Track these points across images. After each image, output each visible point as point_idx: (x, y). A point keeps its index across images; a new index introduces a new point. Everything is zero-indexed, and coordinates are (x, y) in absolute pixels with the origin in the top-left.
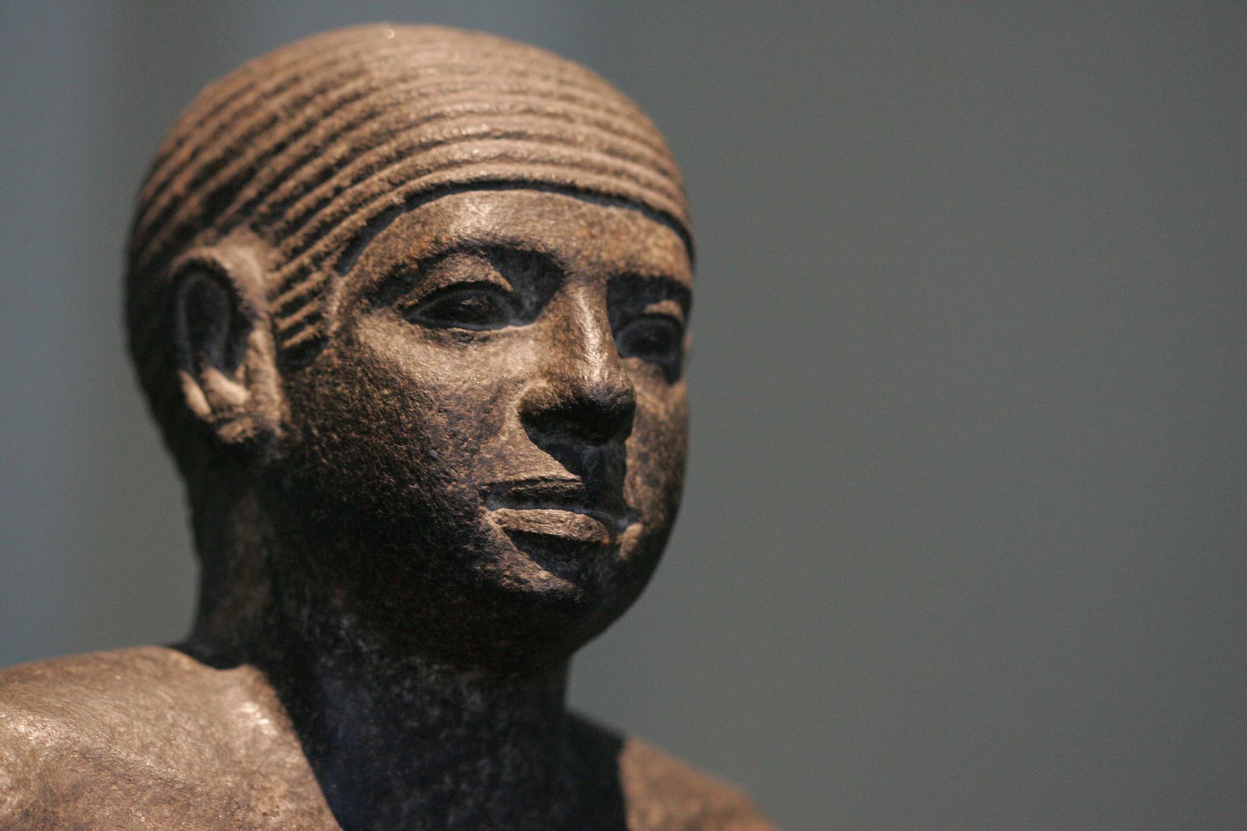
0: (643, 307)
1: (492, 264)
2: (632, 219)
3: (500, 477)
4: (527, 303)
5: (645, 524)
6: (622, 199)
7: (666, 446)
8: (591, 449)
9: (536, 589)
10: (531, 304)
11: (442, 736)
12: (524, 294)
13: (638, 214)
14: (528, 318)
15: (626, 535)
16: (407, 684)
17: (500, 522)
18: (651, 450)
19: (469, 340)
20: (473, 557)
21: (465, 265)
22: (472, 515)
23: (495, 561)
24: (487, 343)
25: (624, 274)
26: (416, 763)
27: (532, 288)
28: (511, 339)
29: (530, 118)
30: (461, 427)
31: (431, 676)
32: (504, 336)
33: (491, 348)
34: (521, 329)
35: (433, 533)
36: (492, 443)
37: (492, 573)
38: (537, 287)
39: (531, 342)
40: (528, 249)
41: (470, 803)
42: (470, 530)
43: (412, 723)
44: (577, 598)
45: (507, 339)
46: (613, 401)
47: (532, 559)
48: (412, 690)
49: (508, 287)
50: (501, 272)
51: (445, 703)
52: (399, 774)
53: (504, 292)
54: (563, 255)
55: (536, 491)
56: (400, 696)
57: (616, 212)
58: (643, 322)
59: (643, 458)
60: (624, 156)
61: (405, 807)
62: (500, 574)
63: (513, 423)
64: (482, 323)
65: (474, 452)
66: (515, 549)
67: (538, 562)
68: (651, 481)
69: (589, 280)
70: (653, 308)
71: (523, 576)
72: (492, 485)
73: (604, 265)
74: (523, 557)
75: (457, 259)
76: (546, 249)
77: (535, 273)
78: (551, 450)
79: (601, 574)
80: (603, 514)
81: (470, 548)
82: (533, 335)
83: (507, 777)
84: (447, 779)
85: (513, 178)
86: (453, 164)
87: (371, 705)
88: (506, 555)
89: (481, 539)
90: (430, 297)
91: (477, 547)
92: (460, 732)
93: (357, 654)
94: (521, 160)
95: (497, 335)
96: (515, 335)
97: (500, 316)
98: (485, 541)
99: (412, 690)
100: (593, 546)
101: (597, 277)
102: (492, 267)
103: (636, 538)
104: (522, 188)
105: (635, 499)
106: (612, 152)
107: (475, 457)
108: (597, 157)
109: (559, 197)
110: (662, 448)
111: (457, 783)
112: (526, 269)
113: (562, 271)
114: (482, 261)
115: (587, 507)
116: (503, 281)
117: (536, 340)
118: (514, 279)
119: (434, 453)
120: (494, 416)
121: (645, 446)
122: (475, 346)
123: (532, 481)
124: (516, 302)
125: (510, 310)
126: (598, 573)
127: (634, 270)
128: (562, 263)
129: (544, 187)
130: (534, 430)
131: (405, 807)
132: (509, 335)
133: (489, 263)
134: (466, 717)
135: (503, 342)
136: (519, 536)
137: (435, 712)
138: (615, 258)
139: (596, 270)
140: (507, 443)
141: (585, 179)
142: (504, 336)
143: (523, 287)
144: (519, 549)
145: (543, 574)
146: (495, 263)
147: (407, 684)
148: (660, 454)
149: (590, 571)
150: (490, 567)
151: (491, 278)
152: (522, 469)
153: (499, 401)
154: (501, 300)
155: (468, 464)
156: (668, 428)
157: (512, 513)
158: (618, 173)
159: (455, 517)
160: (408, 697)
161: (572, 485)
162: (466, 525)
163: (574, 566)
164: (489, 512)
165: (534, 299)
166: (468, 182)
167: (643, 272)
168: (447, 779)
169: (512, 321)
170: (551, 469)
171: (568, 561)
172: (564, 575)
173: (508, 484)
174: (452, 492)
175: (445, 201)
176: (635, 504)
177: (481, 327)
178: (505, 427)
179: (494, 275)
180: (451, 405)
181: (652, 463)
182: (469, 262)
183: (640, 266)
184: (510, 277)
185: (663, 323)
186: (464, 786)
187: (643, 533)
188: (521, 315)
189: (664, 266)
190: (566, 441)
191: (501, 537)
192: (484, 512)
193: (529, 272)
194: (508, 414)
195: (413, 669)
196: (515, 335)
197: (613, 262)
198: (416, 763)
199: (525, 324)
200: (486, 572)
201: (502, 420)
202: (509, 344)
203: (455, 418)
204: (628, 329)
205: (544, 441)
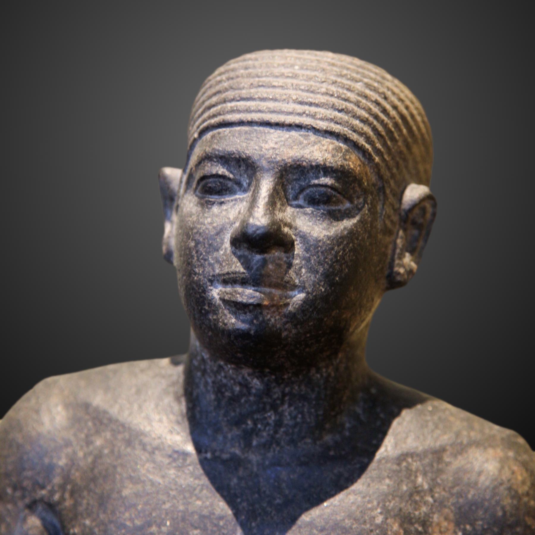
0: (310, 181)
1: (221, 165)
2: (306, 137)
3: (217, 271)
4: (245, 184)
5: (308, 293)
6: (299, 127)
7: (322, 252)
8: (258, 257)
9: (230, 328)
10: (246, 183)
11: (243, 401)
12: (242, 179)
13: (311, 133)
14: (245, 191)
15: (295, 299)
16: (223, 374)
17: (218, 294)
18: (311, 255)
19: (213, 203)
20: (207, 312)
21: (208, 166)
22: (204, 291)
23: (216, 314)
24: (223, 205)
25: (291, 165)
26: (233, 414)
27: (246, 176)
28: (236, 202)
29: (261, 89)
30: (201, 249)
31: (230, 369)
32: (232, 201)
33: (224, 207)
34: (241, 197)
35: (193, 301)
36: (215, 254)
37: (215, 320)
38: (247, 175)
39: (245, 203)
40: (238, 156)
41: (265, 434)
42: (204, 299)
43: (228, 394)
44: (252, 332)
45: (234, 202)
46: (255, 232)
47: (230, 313)
48: (225, 377)
49: (231, 176)
50: (227, 169)
51: (240, 384)
52: (225, 419)
53: (229, 179)
54: (256, 158)
55: (230, 279)
56: (221, 380)
57: (294, 133)
58: (311, 189)
59: (308, 260)
60: (311, 104)
61: (229, 436)
62: (217, 320)
63: (227, 244)
64: (219, 195)
65: (205, 260)
66: (224, 308)
67: (232, 314)
68: (312, 270)
69: (268, 170)
70: (316, 182)
71: (226, 321)
72: (213, 276)
73: (277, 162)
74: (226, 312)
75: (205, 164)
76: (246, 155)
77: (245, 168)
78: (239, 258)
79: (273, 320)
80: (267, 290)
81: (206, 308)
82: (246, 200)
83: (287, 420)
84: (249, 422)
85: (237, 121)
86: (214, 116)
87: (211, 384)
88: (220, 311)
89: (210, 303)
90: (198, 183)
91: (209, 307)
92: (252, 398)
93: (203, 360)
94: (248, 111)
95: (229, 201)
96: (238, 200)
97: (230, 191)
98: (212, 304)
99: (225, 377)
100: (259, 306)
101: (274, 168)
102: (221, 167)
103: (301, 300)
104: (242, 126)
105: (300, 281)
106: (301, 103)
107: (207, 263)
108: (291, 107)
109: (261, 128)
110: (320, 254)
111: (255, 424)
112: (240, 167)
113: (254, 167)
114: (215, 164)
115: (254, 286)
116: (227, 173)
117: (247, 202)
118: (236, 171)
119: (190, 260)
120: (217, 242)
121: (308, 253)
122: (216, 207)
123: (228, 273)
124: (239, 184)
125: (236, 187)
126: (269, 320)
127: (298, 163)
128: (253, 163)
129: (253, 124)
130: (234, 248)
131: (229, 436)
132: (236, 200)
133: (220, 165)
134: (254, 391)
135: (231, 204)
136: (223, 300)
137: (237, 389)
138: (285, 158)
139: (272, 165)
140: (223, 255)
141: (274, 118)
142: (232, 201)
143: (241, 175)
144: (225, 308)
145: (233, 320)
146: (223, 165)
147: (223, 374)
148: (318, 257)
149: (261, 319)
150: (215, 317)
151: (220, 173)
152: (226, 267)
153: (221, 234)
154: (230, 184)
155: (202, 265)
156: (324, 243)
157: (224, 290)
158: (300, 114)
159: (198, 292)
160: (224, 381)
161: (243, 276)
162: (203, 297)
163: (249, 316)
164: (214, 290)
165: (248, 181)
166: (217, 125)
167: (304, 163)
168: (249, 422)
169: (238, 193)
170: (238, 267)
171: (245, 313)
172: (243, 321)
173: (219, 275)
174: (196, 280)
175: (209, 135)
176: (299, 283)
177: (220, 197)
178: (223, 247)
179: (221, 170)
180: (197, 237)
181: (312, 261)
182: (209, 165)
183: (303, 161)
184: (233, 171)
185: (323, 189)
186: (259, 426)
187: (305, 298)
188: (242, 189)
189: (320, 159)
190: (246, 253)
191: (218, 302)
192: (211, 290)
193: (242, 168)
194: (226, 240)
195: (220, 367)
196: (238, 200)
197: (283, 160)
198: (233, 414)
199: (245, 194)
200: (214, 319)
201: (222, 243)
202: (234, 205)
203: (197, 243)
204: (305, 193)
205: (239, 253)
